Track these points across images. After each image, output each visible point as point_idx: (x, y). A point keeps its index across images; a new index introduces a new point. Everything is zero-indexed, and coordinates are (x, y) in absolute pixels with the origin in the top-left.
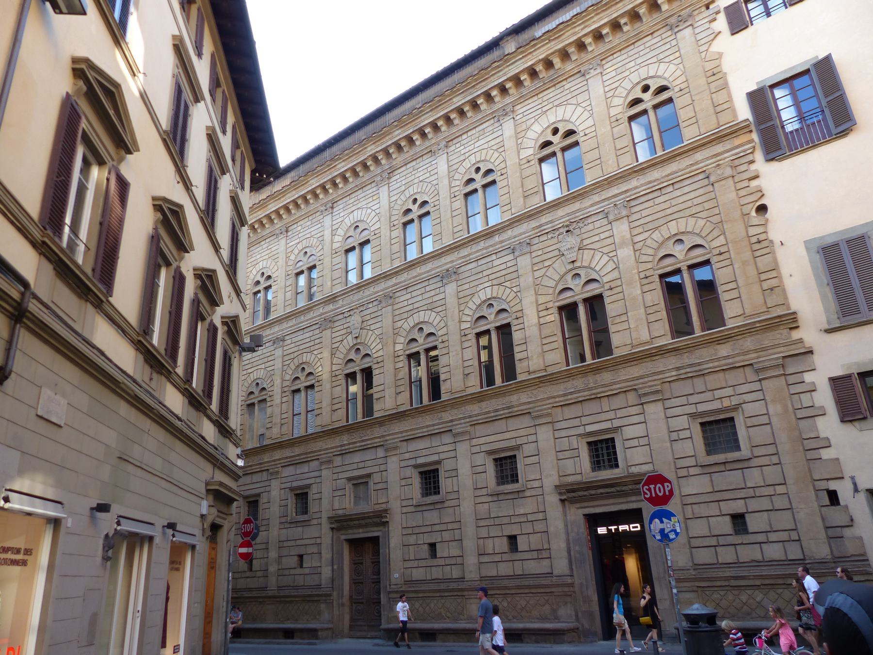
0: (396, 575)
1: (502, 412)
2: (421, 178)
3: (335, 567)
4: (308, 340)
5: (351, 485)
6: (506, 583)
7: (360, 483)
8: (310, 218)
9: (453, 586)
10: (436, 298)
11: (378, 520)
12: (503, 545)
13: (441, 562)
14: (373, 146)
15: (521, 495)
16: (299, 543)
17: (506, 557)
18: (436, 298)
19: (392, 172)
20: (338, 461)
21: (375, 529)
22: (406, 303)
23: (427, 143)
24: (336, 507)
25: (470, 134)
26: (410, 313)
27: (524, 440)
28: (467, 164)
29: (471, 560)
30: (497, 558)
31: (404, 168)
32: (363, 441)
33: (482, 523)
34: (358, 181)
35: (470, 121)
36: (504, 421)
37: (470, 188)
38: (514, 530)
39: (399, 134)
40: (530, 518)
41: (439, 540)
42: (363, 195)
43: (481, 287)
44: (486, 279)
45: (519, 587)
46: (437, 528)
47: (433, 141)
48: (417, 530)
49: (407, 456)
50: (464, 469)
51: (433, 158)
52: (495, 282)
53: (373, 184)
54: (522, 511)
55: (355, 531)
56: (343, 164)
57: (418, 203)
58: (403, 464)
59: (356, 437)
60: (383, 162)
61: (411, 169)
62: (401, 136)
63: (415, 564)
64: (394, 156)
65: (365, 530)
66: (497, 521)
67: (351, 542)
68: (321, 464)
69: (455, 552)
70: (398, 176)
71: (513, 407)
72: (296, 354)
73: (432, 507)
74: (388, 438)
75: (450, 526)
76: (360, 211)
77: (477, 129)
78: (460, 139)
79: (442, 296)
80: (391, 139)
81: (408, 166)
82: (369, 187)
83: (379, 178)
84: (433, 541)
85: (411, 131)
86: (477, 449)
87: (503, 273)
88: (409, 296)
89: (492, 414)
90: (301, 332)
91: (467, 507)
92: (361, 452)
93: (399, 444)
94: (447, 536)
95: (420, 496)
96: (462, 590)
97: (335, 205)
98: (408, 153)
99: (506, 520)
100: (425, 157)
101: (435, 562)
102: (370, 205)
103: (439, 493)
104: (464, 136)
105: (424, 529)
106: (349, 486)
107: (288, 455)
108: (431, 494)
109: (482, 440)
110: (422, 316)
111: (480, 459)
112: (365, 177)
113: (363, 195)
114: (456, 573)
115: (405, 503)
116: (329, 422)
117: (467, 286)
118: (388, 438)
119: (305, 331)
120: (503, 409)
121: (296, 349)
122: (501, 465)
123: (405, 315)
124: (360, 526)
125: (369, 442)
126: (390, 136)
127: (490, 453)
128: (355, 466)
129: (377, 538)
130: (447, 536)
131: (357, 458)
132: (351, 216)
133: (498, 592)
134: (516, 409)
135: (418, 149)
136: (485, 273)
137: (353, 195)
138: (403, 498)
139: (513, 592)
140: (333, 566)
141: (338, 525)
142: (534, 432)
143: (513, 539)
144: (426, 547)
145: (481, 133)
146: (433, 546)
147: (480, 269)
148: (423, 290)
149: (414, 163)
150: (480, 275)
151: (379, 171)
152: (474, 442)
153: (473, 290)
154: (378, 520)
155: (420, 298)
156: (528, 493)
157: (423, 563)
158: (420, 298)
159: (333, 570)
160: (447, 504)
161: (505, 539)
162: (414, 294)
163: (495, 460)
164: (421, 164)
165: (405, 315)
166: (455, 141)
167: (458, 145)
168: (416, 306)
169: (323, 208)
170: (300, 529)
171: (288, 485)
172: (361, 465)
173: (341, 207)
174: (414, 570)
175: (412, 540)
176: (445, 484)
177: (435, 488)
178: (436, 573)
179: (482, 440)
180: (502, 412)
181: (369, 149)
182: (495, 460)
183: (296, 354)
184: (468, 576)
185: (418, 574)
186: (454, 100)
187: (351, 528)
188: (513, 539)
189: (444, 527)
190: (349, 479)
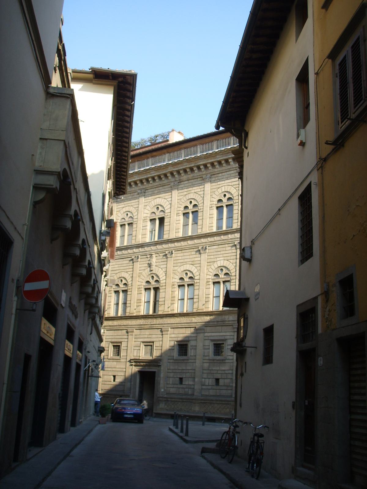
0: (162, 390)
1: (220, 323)
2: (196, 191)
3: (132, 383)
4: (125, 265)
6: (212, 398)
8: (132, 194)
9: (189, 397)
10: (196, 259)
11: (156, 364)
12: (212, 382)
13: (185, 386)
14: (172, 168)
15: (224, 361)
16: (114, 369)
17: (215, 387)
18: (196, 259)
19: (180, 181)
21: (154, 368)
22: (180, 258)
23: (201, 173)
25: (223, 174)
26: (182, 264)
27: (228, 337)
28: (220, 191)
29: (197, 387)
30: (210, 387)
31: (187, 182)
33: (205, 372)
34: (161, 183)
35: (223, 168)
36: (221, 327)
37: (220, 205)
38: (218, 376)
39: (186, 165)
40: (226, 372)
41: (185, 376)
42: (163, 190)
43: (218, 259)
44: (222, 256)
45: (217, 400)
46: (185, 371)
47: (204, 173)
48: (174, 371)
49: (173, 336)
50: (200, 345)
51: (203, 181)
52: (225, 258)
53: (169, 186)
54: (223, 369)
56: (154, 172)
57: (193, 204)
58: (171, 339)
59: (149, 321)
60: (176, 176)
61: (191, 184)
62: (187, 166)
63: (172, 386)
64: (182, 175)
66: (212, 372)
69: (191, 383)
70: (183, 186)
71: (226, 321)
72: (118, 271)
73: (183, 361)
75: (190, 371)
76: (160, 199)
77: (227, 173)
78: (218, 175)
79: (199, 259)
80: (182, 166)
81: (190, 181)
82: (167, 186)
83: (172, 184)
84: (181, 377)
85: (193, 165)
86: (207, 338)
87: (230, 255)
88: (182, 254)
89: (215, 323)
90: (122, 260)
91: (198, 363)
94: (188, 375)
95: (177, 355)
96: (192, 399)
97: (147, 191)
98: (191, 175)
99: (215, 372)
100: (199, 179)
101: (181, 386)
102: (166, 197)
103: (187, 355)
104: (220, 175)
105: (177, 371)
107: (110, 324)
108: (183, 355)
109: (209, 334)
110: (188, 267)
111: (207, 343)
112: (165, 181)
113: (163, 190)
114: (190, 392)
115: (170, 358)
117: (212, 257)
119: (124, 259)
120: (221, 321)
121: (118, 268)
122: (217, 347)
123: (179, 264)
125: (155, 326)
126: (182, 165)
127: (212, 340)
128: (146, 336)
129: (154, 372)
130: (188, 375)
131: (147, 332)
132: (155, 200)
133: (208, 402)
134: (227, 322)
135: (195, 175)
136: (221, 252)
137: (157, 189)
138: (169, 355)
139: (214, 402)
140: (131, 383)
142: (233, 334)
143: (217, 380)
144: (178, 379)
145: (229, 176)
146: (181, 379)
147: (219, 250)
148: (190, 253)
149: (193, 181)
150: (219, 253)
151: (173, 180)
152: (206, 334)
153: (215, 260)
154: (156, 364)
155: (188, 257)
156: (227, 361)
157: (175, 386)
158: (188, 257)
159: (131, 385)
160: (190, 361)
161: (214, 379)
162: (185, 254)
163: (214, 344)
164: (196, 183)
165: (179, 264)
166: (215, 176)
167: (216, 178)
168: (186, 260)
169: (139, 191)
170: (115, 363)
171: (110, 340)
172: (150, 336)
173: (150, 193)
174: (171, 389)
175: (172, 375)
176: (191, 352)
177: (185, 352)
178: (181, 391)
179: (209, 334)
180: (220, 323)
181: (169, 168)
182: (214, 344)
183: (118, 271)
184: (195, 394)
185: (172, 390)
186: (217, 156)
188: (217, 380)
189: (187, 371)
190: (143, 342)
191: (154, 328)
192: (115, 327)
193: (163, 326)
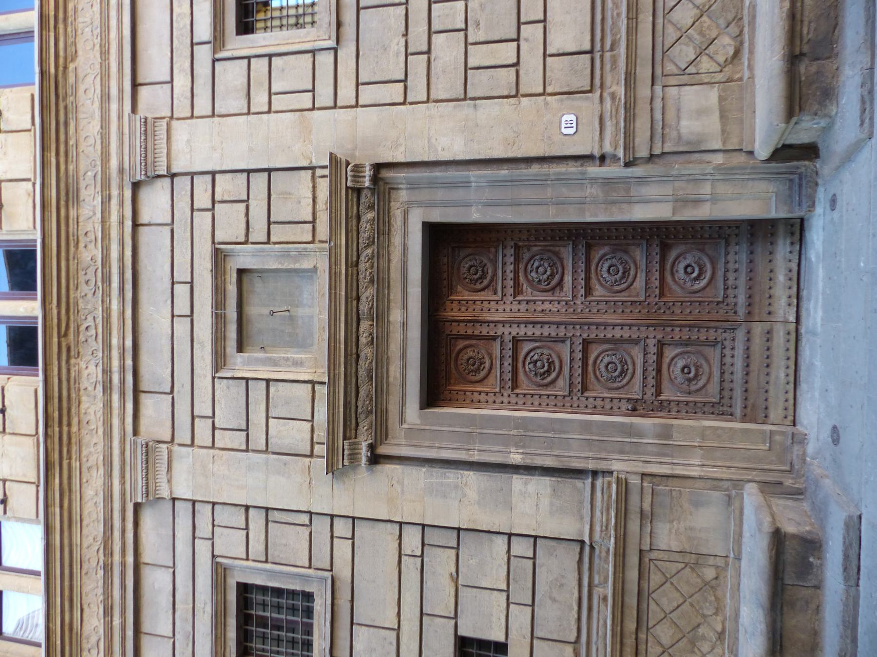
5: (239, 358)
7: (238, 306)
20: (154, 410)
24: (295, 435)
32: (107, 279)
55: (394, 348)
65: (396, 294)
67: (434, 394)
68: (152, 498)
74: (114, 163)
92: (143, 296)
93: (142, 111)
106: (240, 365)
116: (30, 442)
118: (114, 163)
124: (380, 316)
128: (182, 327)
141: (364, 425)
187: (381, 360)
190: (220, 360)
191: (128, 253)
192: (117, 622)
193: (121, 171)
